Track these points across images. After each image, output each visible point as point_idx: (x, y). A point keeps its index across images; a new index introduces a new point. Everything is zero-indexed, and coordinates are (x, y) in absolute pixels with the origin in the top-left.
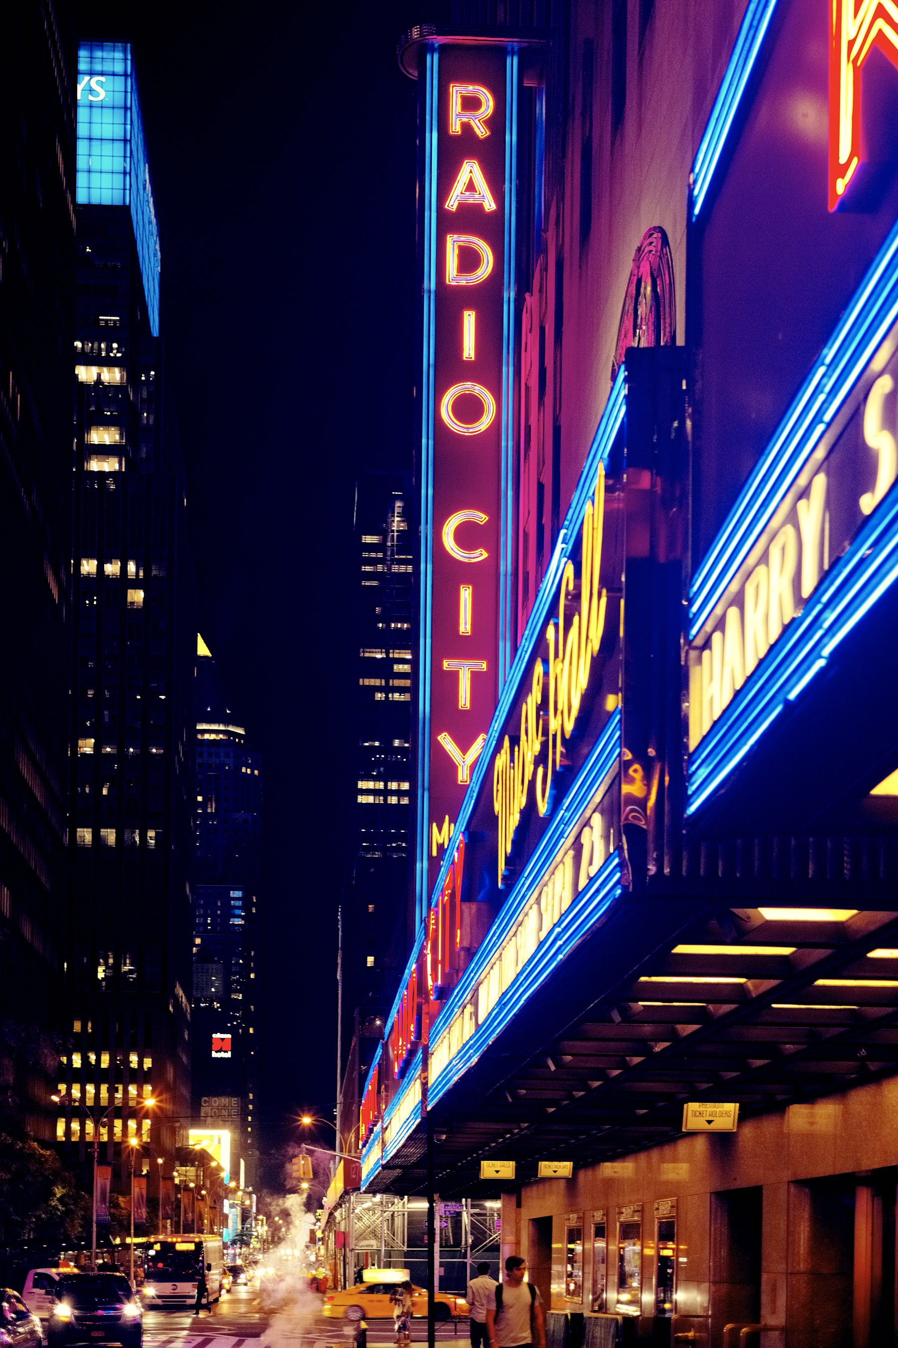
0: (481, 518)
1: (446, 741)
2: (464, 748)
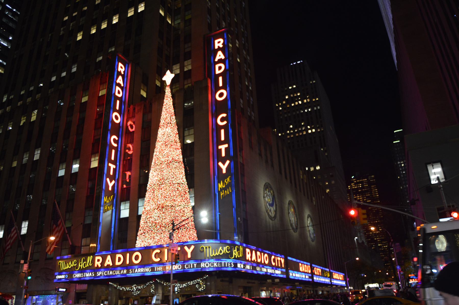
0: (117, 139)
1: (108, 180)
2: (111, 182)
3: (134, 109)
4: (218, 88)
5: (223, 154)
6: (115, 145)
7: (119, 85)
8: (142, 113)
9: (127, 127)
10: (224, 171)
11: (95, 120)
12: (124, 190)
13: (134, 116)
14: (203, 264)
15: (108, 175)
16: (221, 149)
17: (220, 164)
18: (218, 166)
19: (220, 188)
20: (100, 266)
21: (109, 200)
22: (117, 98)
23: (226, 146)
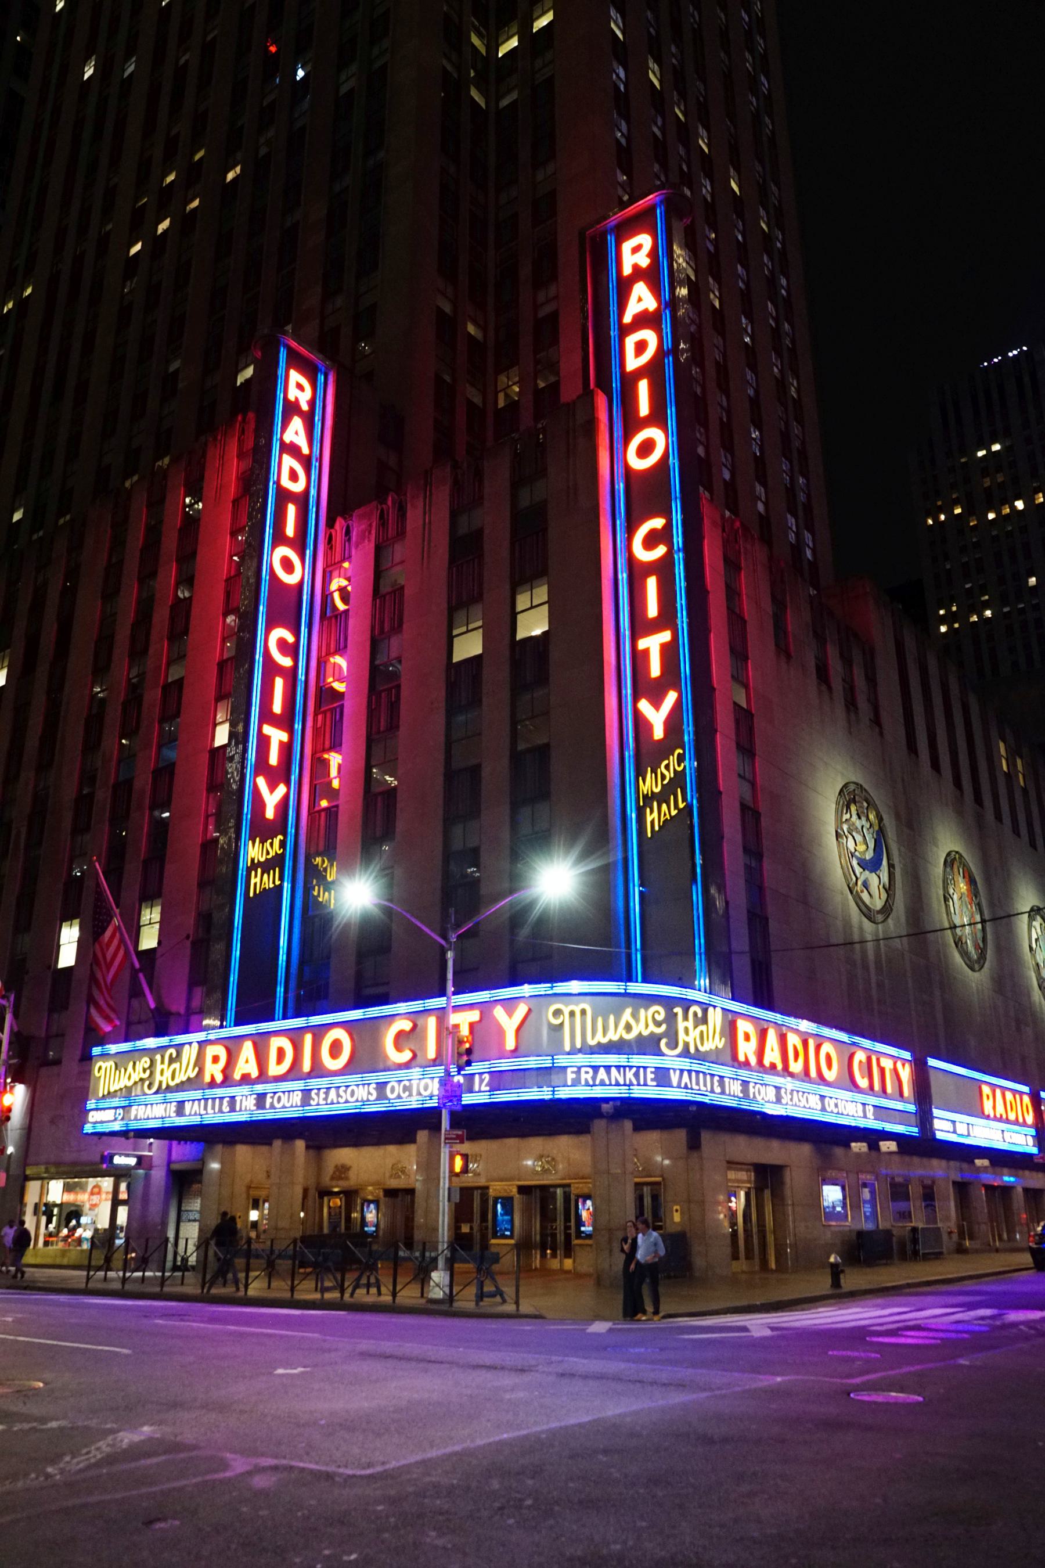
0: (291, 639)
1: (261, 781)
2: (272, 788)
3: (348, 532)
4: (632, 424)
5: (655, 671)
6: (286, 662)
7: (292, 449)
8: (373, 545)
9: (327, 596)
10: (658, 733)
11: (226, 581)
12: (320, 816)
13: (346, 556)
14: (587, 1072)
15: (262, 766)
16: (646, 652)
17: (644, 706)
18: (637, 713)
19: (645, 797)
20: (219, 1078)
21: (268, 853)
22: (284, 496)
23: (666, 636)
